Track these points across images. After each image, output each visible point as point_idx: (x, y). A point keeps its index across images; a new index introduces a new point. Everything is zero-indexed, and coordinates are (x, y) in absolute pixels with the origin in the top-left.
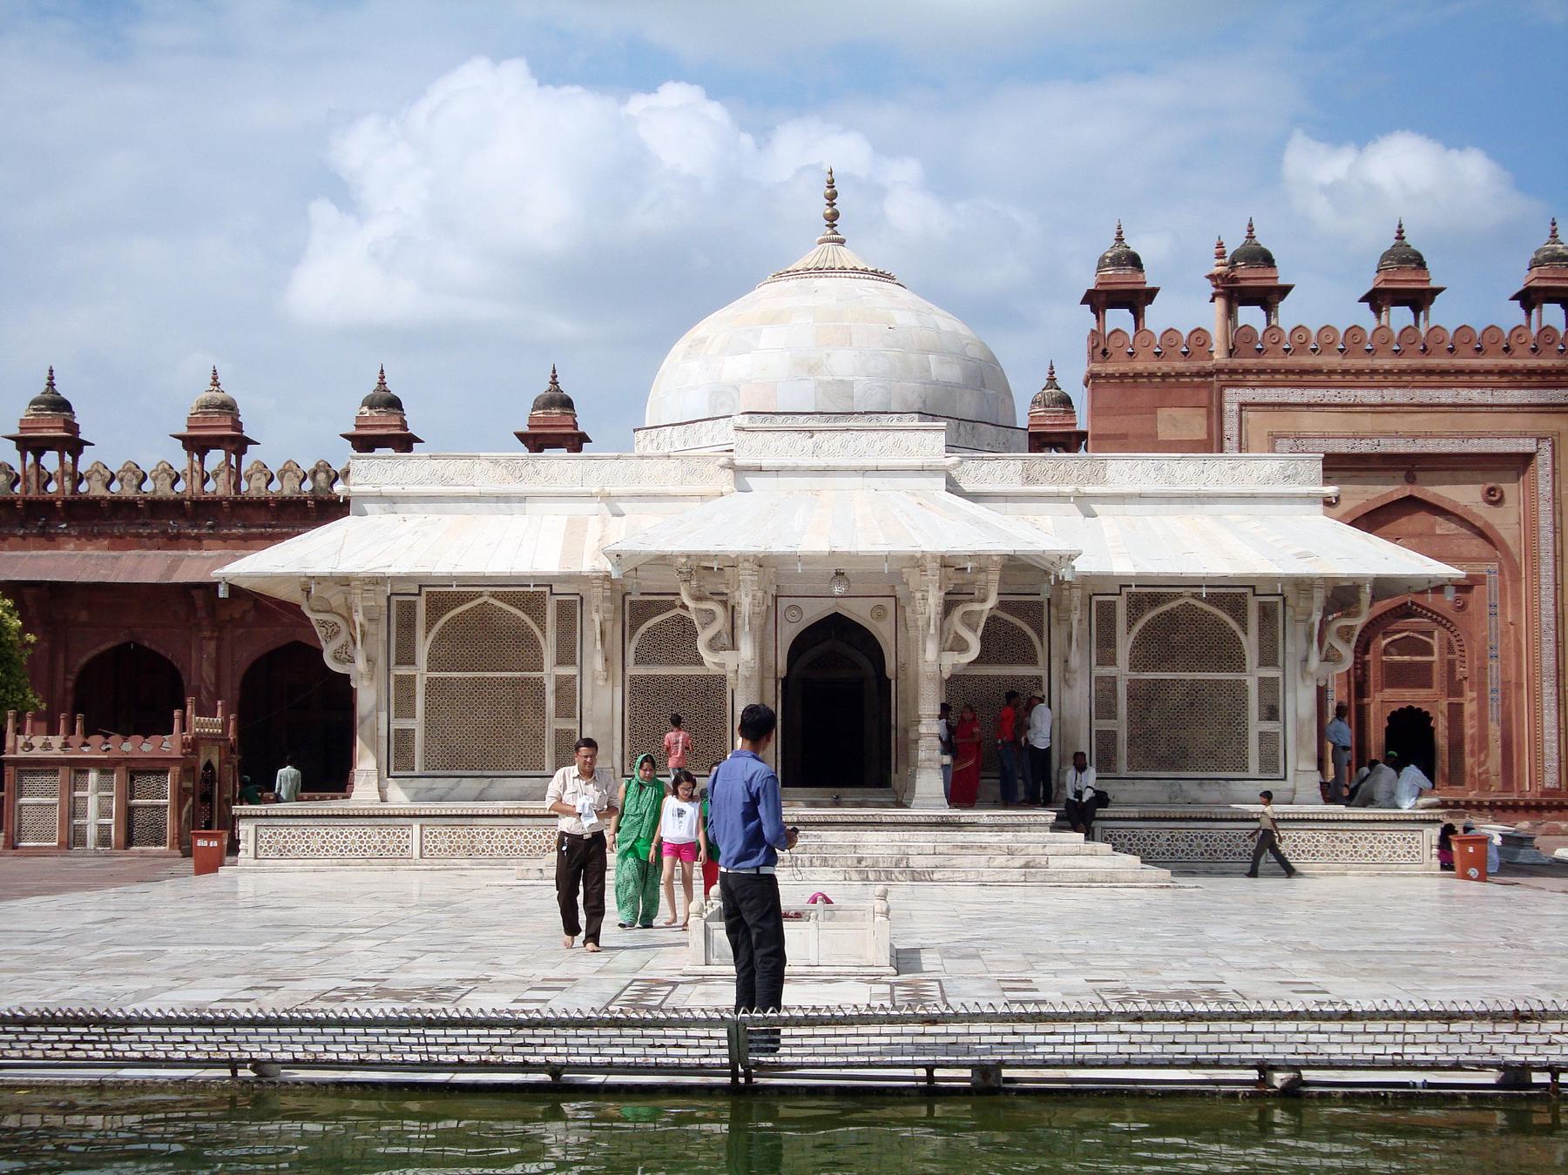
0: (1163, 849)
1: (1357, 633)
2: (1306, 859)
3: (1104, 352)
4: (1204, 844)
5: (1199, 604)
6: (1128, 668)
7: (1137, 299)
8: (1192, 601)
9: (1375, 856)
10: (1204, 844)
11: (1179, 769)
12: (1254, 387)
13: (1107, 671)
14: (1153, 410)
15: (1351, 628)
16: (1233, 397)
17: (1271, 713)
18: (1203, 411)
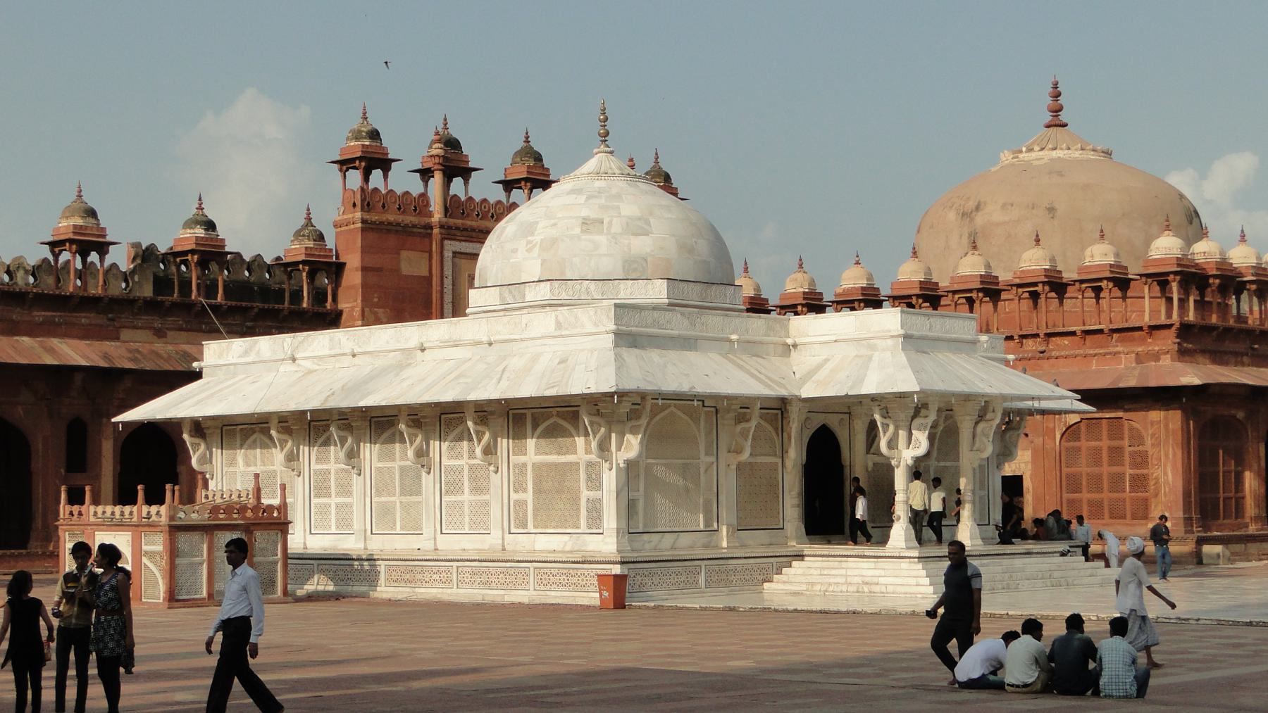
3: (368, 203)
12: (460, 241)
14: (399, 254)
16: (451, 246)
18: (427, 255)
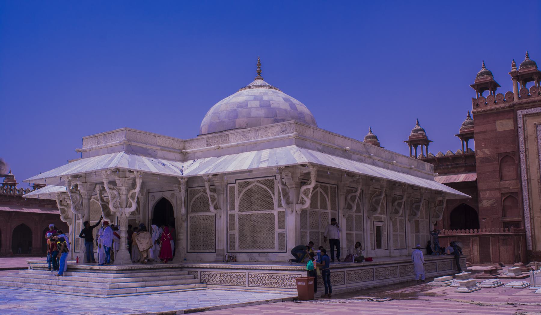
0: (217, 280)
2: (262, 285)
4: (230, 278)
5: (260, 185)
6: (238, 211)
7: (494, 86)
8: (257, 184)
9: (285, 285)
10: (230, 278)
11: (254, 248)
12: (528, 109)
13: (232, 212)
15: (309, 189)
17: (282, 225)
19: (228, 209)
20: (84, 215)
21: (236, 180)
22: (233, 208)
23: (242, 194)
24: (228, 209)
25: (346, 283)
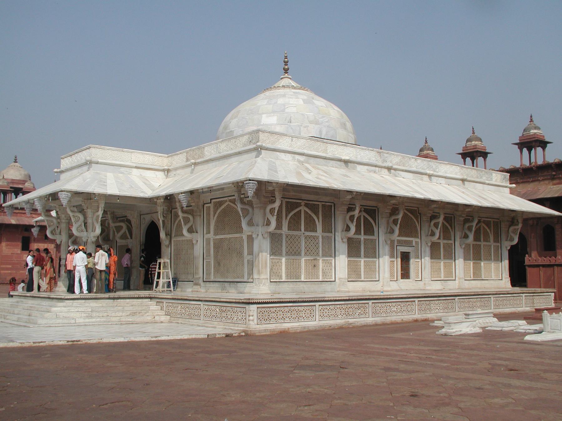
0: (179, 312)
1: (276, 211)
6: (213, 235)
19: (205, 232)
20: (62, 240)
21: (211, 200)
22: (208, 232)
23: (216, 216)
24: (205, 232)
25: (317, 320)
